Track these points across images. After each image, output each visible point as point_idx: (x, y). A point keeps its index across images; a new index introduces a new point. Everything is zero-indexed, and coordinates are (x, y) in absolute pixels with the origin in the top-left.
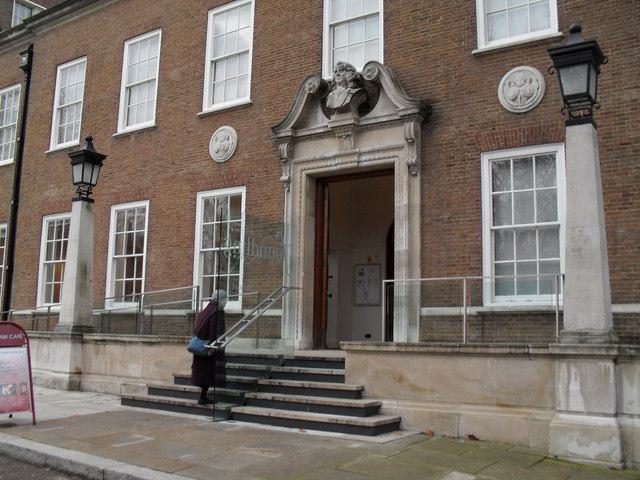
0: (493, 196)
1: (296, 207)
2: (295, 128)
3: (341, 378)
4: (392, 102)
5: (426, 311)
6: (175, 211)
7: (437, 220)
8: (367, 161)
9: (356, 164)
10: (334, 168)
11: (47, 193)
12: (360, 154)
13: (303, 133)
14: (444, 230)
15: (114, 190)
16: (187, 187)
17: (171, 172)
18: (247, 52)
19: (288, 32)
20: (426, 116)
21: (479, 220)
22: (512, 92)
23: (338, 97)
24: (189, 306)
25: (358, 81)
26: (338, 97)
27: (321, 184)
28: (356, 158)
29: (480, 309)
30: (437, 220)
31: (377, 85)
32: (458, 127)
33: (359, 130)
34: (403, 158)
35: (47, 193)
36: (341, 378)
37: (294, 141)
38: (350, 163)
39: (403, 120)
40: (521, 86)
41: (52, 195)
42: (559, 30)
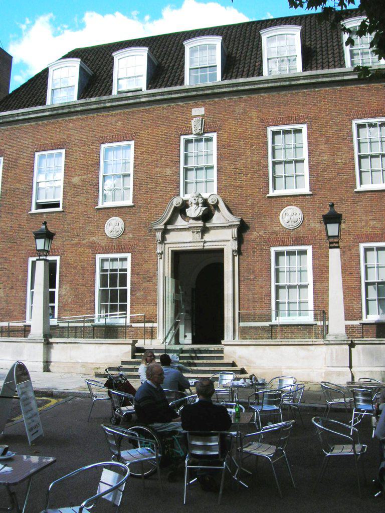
0: (276, 268)
1: (164, 267)
2: (166, 224)
3: (222, 358)
4: (222, 217)
5: (242, 324)
7: (248, 279)
8: (208, 246)
9: (202, 247)
12: (205, 242)
13: (169, 227)
14: (251, 284)
17: (76, 241)
18: (129, 175)
19: (157, 167)
20: (243, 228)
21: (270, 280)
22: (287, 218)
23: (194, 211)
24: (93, 321)
25: (205, 203)
26: (194, 211)
27: (177, 256)
28: (202, 244)
29: (270, 323)
30: (248, 279)
31: (216, 206)
32: (258, 233)
33: (204, 230)
34: (230, 247)
36: (222, 358)
37: (165, 232)
38: (199, 246)
39: (230, 226)
40: (290, 216)
42: (310, 191)
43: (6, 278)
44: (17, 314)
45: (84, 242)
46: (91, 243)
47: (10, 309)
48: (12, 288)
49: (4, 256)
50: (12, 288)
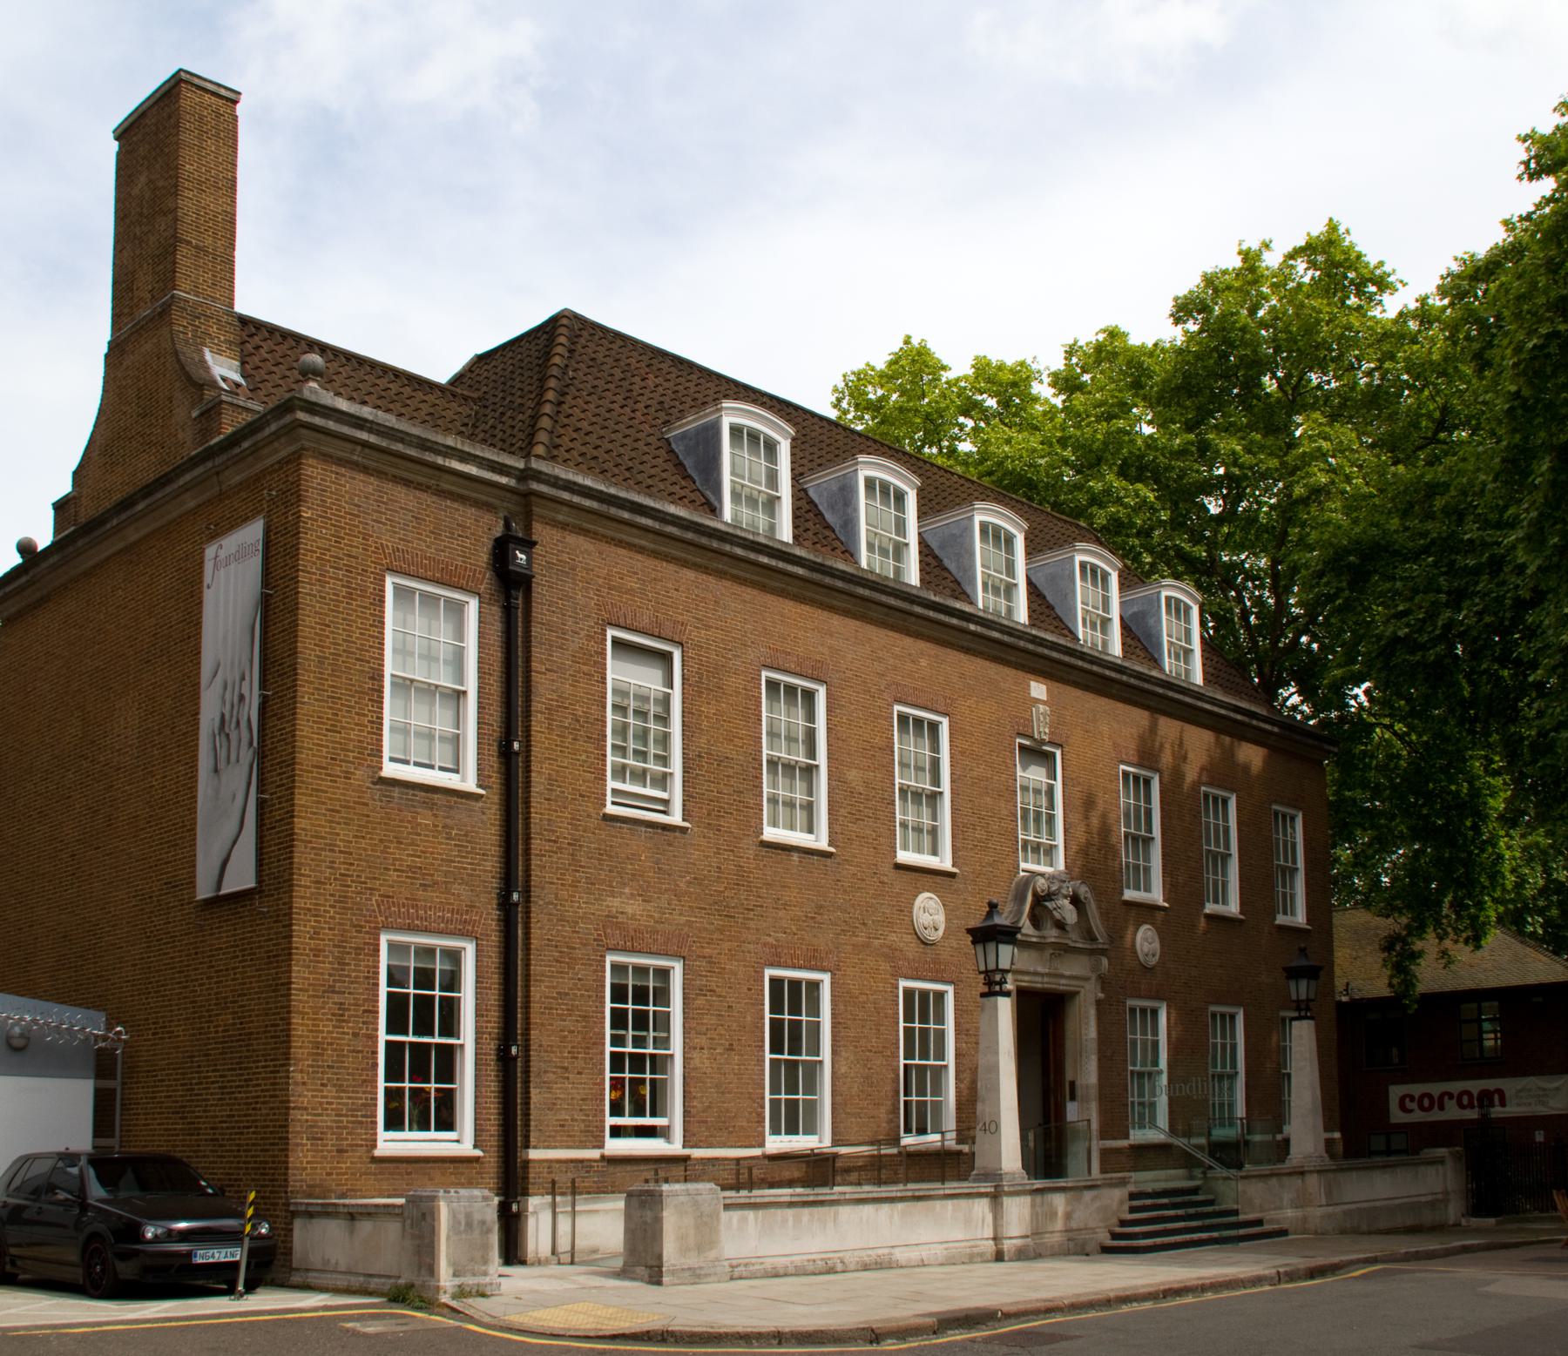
6: (871, 998)
10: (1039, 986)
11: (615, 903)
15: (770, 940)
16: (885, 966)
35: (615, 903)
41: (629, 910)
43: (714, 1020)
44: (744, 1124)
45: (876, 942)
46: (890, 947)
47: (727, 1111)
48: (730, 1048)
49: (707, 951)
50: (730, 1048)
